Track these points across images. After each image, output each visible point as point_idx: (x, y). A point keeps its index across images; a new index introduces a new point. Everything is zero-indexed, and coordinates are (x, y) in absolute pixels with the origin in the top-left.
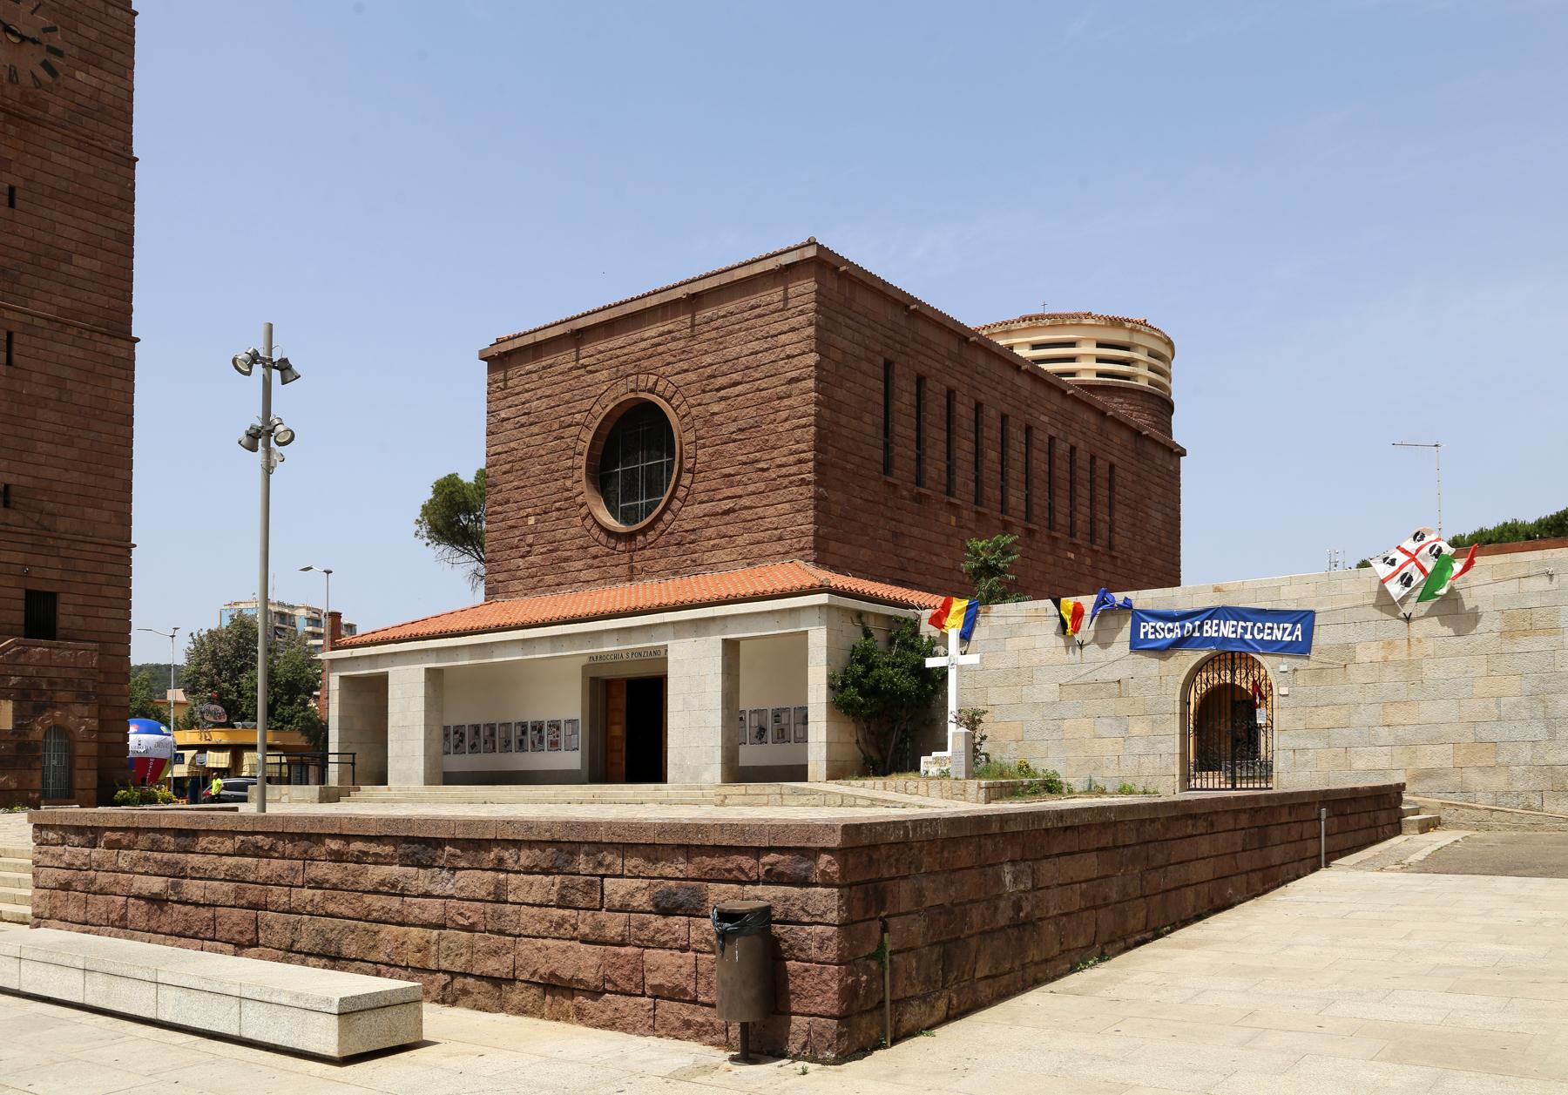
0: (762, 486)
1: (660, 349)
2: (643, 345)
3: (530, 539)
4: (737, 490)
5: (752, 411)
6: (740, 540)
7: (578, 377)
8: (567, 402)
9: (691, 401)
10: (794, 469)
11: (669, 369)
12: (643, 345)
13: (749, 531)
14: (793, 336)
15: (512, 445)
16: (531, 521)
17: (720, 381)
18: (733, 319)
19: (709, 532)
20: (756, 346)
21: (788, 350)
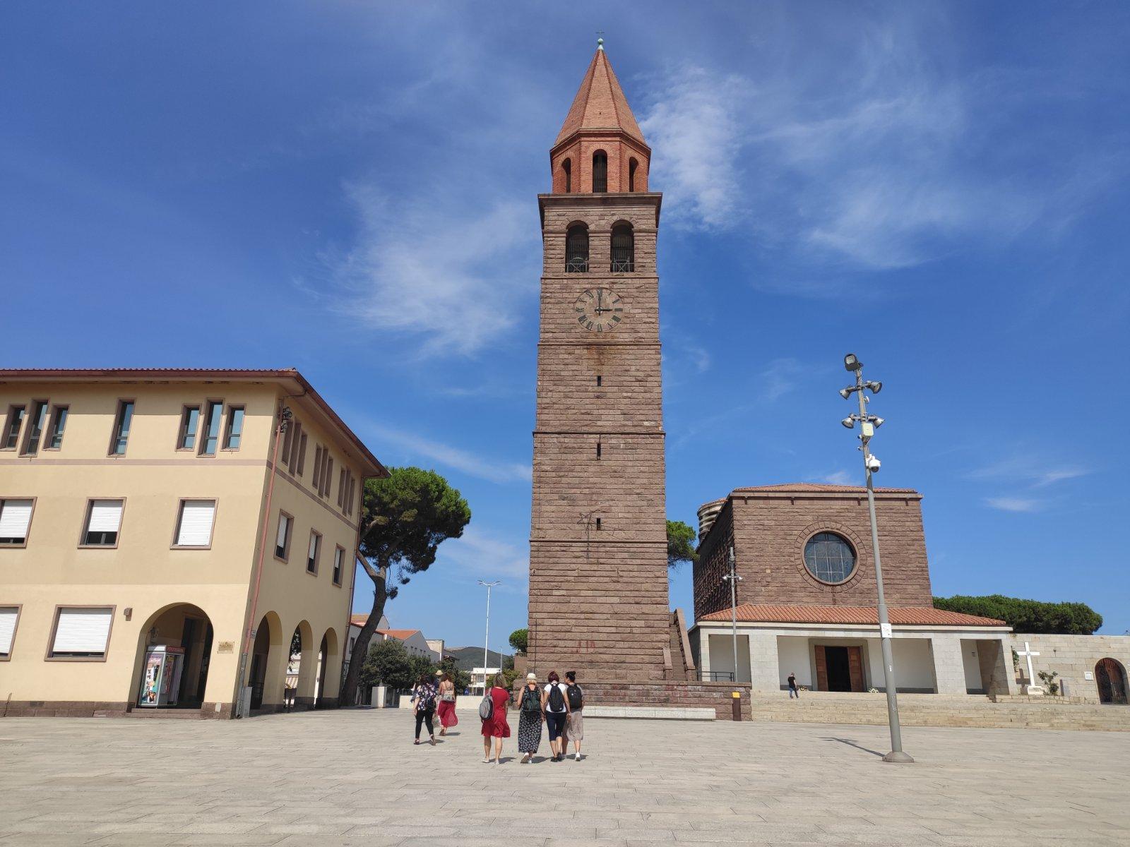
0: (904, 577)
2: (832, 511)
3: (769, 579)
4: (893, 577)
11: (848, 523)
12: (832, 511)
15: (753, 537)
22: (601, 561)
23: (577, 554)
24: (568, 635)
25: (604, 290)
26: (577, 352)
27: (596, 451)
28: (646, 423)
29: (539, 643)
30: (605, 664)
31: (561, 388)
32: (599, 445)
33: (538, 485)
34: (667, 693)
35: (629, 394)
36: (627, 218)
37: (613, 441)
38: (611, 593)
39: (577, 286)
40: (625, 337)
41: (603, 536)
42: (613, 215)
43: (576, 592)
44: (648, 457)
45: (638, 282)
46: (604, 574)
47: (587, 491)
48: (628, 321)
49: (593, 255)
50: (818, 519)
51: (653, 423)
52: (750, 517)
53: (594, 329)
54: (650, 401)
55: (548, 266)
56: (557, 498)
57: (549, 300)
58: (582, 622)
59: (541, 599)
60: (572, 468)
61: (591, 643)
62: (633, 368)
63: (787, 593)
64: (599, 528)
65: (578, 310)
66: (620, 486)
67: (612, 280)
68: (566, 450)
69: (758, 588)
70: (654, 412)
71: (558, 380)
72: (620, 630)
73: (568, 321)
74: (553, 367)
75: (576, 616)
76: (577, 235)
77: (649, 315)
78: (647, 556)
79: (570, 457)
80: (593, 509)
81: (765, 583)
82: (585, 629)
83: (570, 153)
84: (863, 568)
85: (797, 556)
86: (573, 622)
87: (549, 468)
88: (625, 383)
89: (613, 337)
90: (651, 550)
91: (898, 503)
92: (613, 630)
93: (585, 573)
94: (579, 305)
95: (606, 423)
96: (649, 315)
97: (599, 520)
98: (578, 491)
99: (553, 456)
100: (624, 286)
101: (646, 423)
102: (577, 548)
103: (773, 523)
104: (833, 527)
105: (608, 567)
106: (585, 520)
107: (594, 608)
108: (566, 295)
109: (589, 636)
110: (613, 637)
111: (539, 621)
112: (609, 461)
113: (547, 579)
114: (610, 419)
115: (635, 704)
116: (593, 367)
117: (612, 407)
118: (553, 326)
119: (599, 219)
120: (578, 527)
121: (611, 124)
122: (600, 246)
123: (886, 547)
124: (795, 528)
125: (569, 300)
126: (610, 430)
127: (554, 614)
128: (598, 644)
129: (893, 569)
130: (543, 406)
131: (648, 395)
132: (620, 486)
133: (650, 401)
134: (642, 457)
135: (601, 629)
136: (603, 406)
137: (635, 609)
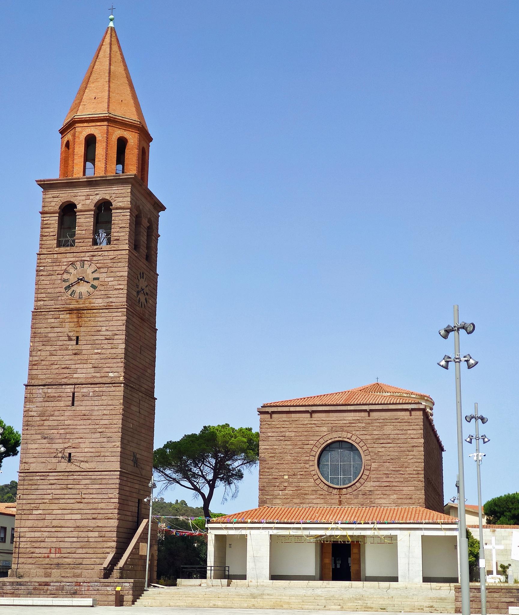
0: (402, 480)
1: (353, 425)
2: (345, 422)
3: (286, 484)
4: (391, 480)
5: (396, 454)
6: (392, 497)
7: (312, 427)
8: (305, 436)
9: (368, 445)
10: (416, 476)
12: (345, 422)
13: (396, 494)
14: (415, 432)
15: (275, 447)
16: (286, 477)
17: (382, 441)
18: (388, 421)
19: (378, 492)
20: (398, 432)
21: (412, 436)
22: (70, 486)
23: (52, 482)
24: (42, 545)
25: (86, 262)
26: (61, 316)
27: (71, 399)
28: (111, 375)
29: (21, 550)
30: (67, 566)
31: (48, 348)
32: (74, 394)
33: (26, 428)
34: (76, 588)
35: (99, 351)
36: (108, 197)
37: (85, 390)
38: (75, 512)
39: (65, 260)
40: (99, 302)
41: (72, 467)
42: (97, 194)
43: (50, 511)
44: (110, 402)
46: (71, 496)
47: (62, 431)
48: (102, 288)
49: (79, 232)
50: (332, 430)
51: (116, 374)
52: (274, 430)
53: (77, 295)
54: (115, 355)
55: (43, 242)
56: (40, 438)
57: (42, 273)
58: (52, 534)
59: (24, 517)
60: (52, 413)
61: (59, 550)
62: (104, 329)
63: (300, 495)
64: (69, 461)
65: (65, 281)
66: (88, 427)
67: (92, 253)
68: (48, 398)
69: (276, 493)
70: (118, 365)
71: (46, 341)
72: (80, 539)
73: (57, 290)
74: (42, 330)
75: (48, 529)
76: (68, 211)
77: (120, 282)
78: (104, 481)
79: (52, 404)
80: (66, 445)
81: (283, 488)
82: (54, 540)
83: (69, 137)
84: (367, 473)
85: (311, 463)
86: (46, 534)
87: (35, 414)
88: (97, 342)
89: (90, 303)
90: (107, 477)
91: (403, 413)
92: (75, 539)
93: (57, 496)
94: (65, 276)
95: (80, 376)
96: (120, 282)
97: (70, 454)
98: (56, 431)
99: (39, 404)
100: (101, 258)
101: (111, 375)
102: (52, 477)
103: (293, 434)
104: (344, 436)
105: (74, 491)
106: (60, 455)
107: (62, 523)
108: (55, 268)
109: (57, 545)
110: (74, 545)
111: (22, 534)
112: (81, 407)
113: (29, 501)
114: (83, 373)
115: (54, 596)
116: (73, 329)
117: (85, 362)
118: (44, 295)
119: (85, 200)
120: (54, 460)
121: (101, 111)
122: (85, 222)
123: (389, 453)
124: (312, 438)
125: (57, 272)
126: (83, 381)
128: (64, 551)
129: (393, 473)
130: (33, 363)
131: (113, 351)
132: (88, 427)
133: (115, 355)
134: (105, 403)
135: (66, 539)
136: (79, 362)
137: (92, 523)
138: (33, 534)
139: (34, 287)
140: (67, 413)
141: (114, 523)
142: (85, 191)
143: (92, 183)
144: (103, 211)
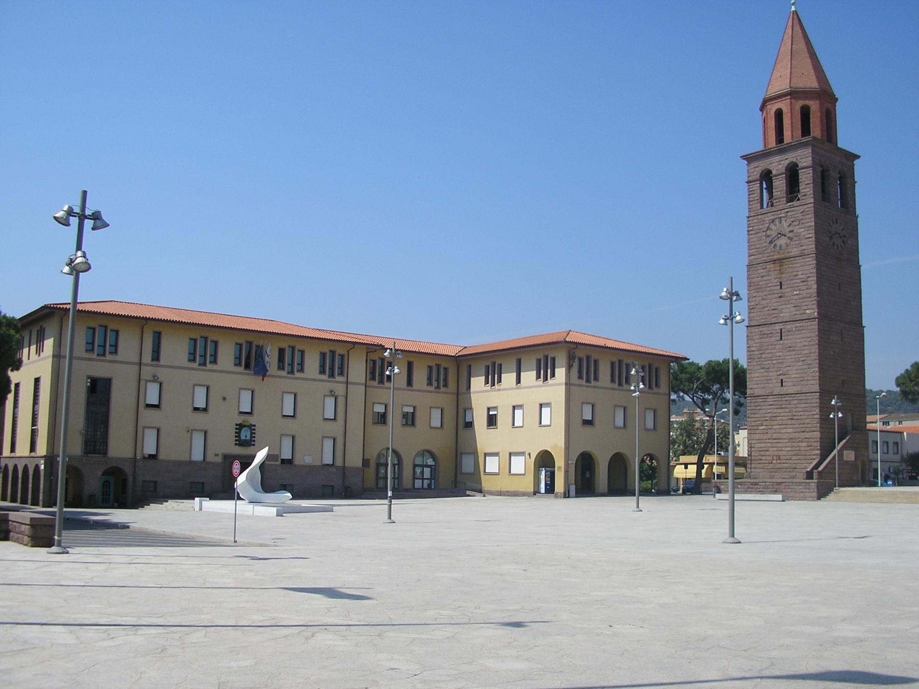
31: (760, 294)
37: (789, 326)
40: (795, 251)
44: (808, 335)
45: (801, 209)
48: (795, 238)
59: (753, 432)
62: (800, 273)
65: (768, 236)
68: (763, 335)
79: (767, 340)
86: (769, 445)
94: (769, 232)
101: (808, 311)
102: (770, 399)
105: (787, 410)
107: (780, 436)
110: (790, 453)
112: (787, 341)
127: (760, 440)
131: (809, 291)
138: (760, 445)
139: (747, 244)
140: (777, 347)
141: (817, 435)
142: (777, 158)
143: (781, 151)
144: (792, 173)
